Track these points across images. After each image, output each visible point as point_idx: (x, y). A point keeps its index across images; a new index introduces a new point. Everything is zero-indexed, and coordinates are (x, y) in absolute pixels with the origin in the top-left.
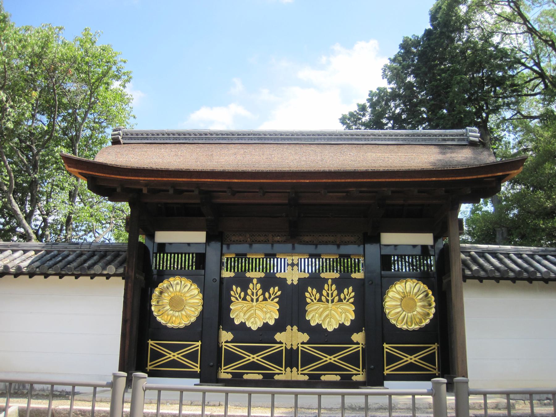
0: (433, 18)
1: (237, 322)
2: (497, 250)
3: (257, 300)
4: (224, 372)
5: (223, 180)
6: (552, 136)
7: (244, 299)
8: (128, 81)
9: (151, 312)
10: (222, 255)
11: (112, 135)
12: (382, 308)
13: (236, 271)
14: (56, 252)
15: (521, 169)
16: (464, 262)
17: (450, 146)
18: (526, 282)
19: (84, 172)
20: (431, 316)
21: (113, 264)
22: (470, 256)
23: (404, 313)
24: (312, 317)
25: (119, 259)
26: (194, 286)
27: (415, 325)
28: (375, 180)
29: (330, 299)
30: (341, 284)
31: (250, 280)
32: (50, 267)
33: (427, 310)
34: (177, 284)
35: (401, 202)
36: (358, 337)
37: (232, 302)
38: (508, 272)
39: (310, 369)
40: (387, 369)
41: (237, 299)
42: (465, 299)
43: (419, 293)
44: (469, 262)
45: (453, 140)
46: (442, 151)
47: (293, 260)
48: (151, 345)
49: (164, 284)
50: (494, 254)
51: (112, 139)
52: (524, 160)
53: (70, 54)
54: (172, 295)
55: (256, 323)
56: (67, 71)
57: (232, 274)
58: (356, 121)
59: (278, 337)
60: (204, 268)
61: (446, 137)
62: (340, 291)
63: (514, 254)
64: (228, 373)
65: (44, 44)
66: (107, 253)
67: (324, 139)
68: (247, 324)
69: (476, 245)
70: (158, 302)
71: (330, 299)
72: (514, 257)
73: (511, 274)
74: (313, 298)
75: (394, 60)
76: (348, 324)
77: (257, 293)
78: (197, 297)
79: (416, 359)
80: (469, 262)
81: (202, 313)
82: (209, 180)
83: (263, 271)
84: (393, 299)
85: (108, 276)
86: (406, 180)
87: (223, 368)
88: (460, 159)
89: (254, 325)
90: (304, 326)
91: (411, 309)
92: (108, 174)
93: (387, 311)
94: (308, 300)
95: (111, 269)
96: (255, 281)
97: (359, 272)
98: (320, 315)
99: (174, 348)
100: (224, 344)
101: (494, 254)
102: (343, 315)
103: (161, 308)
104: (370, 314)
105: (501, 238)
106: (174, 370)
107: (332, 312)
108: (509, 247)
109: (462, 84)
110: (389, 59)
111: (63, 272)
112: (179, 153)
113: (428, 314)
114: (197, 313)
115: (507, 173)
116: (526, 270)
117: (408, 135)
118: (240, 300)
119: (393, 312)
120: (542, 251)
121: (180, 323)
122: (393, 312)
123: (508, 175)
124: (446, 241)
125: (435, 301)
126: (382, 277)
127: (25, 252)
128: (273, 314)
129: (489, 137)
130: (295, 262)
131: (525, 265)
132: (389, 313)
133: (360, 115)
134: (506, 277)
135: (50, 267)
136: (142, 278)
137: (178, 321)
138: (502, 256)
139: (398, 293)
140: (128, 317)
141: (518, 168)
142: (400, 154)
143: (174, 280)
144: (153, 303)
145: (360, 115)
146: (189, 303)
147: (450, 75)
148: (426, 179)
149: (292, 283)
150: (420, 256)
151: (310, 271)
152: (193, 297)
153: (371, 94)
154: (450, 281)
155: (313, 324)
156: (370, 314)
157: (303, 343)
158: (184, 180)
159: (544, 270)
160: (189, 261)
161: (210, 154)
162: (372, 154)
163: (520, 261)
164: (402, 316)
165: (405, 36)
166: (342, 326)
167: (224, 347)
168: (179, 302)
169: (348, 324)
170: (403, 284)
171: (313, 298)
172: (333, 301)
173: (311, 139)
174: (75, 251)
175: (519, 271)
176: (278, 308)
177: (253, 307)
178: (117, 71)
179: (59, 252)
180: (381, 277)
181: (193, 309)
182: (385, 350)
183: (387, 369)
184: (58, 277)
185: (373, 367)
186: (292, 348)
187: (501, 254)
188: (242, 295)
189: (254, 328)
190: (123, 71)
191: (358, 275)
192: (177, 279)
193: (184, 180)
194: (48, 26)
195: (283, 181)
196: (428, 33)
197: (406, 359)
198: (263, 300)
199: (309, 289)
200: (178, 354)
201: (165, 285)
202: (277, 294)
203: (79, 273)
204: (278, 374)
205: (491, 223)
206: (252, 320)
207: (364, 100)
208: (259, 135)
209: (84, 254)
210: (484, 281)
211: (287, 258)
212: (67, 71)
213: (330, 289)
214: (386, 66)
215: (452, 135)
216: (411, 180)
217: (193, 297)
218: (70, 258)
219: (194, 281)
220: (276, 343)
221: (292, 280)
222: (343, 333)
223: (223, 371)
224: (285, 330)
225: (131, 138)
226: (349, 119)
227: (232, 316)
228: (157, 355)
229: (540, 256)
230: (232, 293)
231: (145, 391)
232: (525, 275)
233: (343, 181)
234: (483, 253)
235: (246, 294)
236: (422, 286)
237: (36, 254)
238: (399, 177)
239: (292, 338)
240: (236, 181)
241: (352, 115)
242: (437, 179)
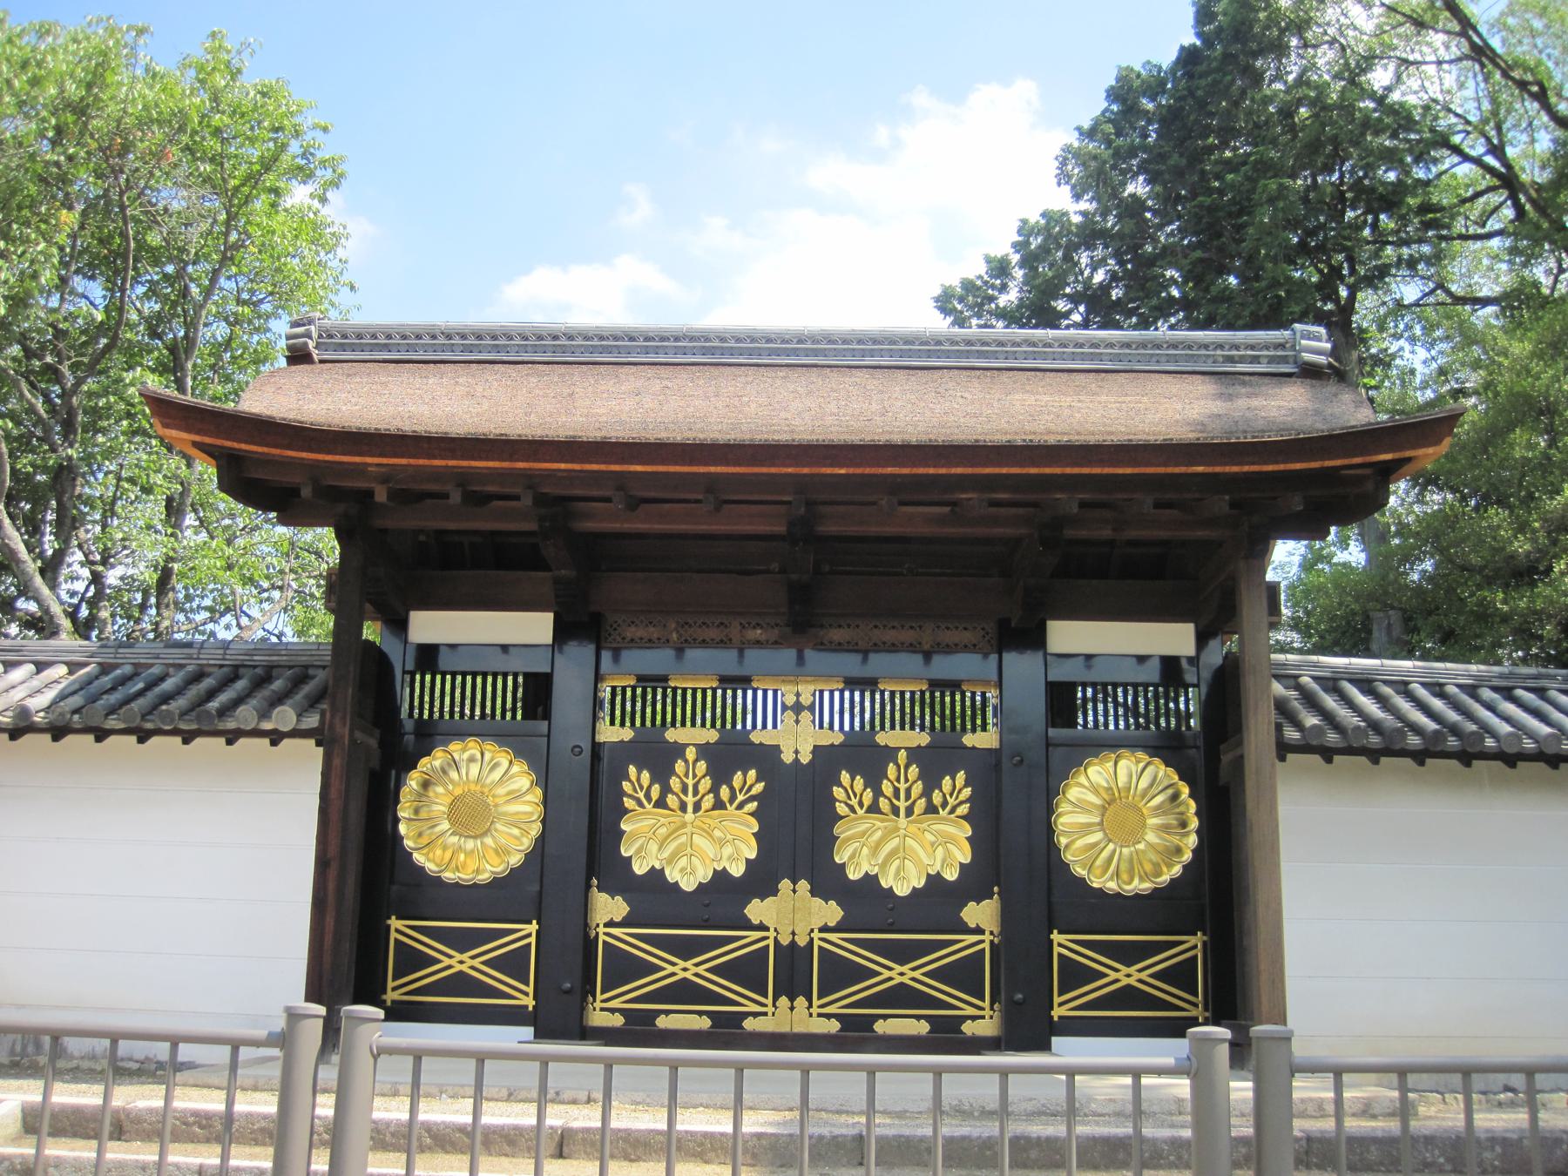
0: (1204, 15)
1: (639, 868)
2: (1376, 671)
3: (697, 807)
4: (602, 1009)
5: (603, 467)
6: (1533, 355)
7: (661, 803)
8: (335, 184)
9: (397, 838)
10: (598, 678)
11: (288, 338)
12: (1050, 831)
13: (638, 723)
14: (128, 669)
15: (1447, 441)
16: (1281, 707)
17: (1247, 378)
18: (1454, 764)
19: (207, 440)
20: (1187, 856)
21: (290, 701)
22: (1299, 687)
23: (1111, 846)
24: (852, 857)
25: (307, 689)
26: (519, 767)
27: (1141, 880)
28: (1034, 471)
29: (902, 805)
30: (935, 762)
31: (678, 750)
32: (112, 711)
33: (1175, 840)
34: (472, 760)
35: (1106, 533)
36: (982, 914)
37: (626, 811)
38: (1404, 736)
39: (843, 1001)
40: (1060, 1005)
41: (640, 804)
42: (1284, 810)
43: (1154, 790)
44: (1296, 704)
45: (1255, 360)
46: (1224, 390)
47: (798, 695)
48: (397, 931)
49: (434, 761)
50: (1366, 684)
51: (289, 348)
52: (1453, 419)
53: (167, 106)
54: (458, 791)
55: (693, 872)
56: (159, 155)
57: (627, 734)
58: (982, 304)
59: (756, 910)
60: (547, 716)
61: (1235, 353)
62: (931, 781)
63: (1423, 684)
64: (613, 1011)
65: (94, 74)
66: (275, 672)
67: (891, 353)
68: (667, 873)
69: (1314, 658)
70: (417, 811)
71: (902, 805)
72: (1422, 693)
73: (1414, 741)
74: (854, 802)
75: (1090, 134)
76: (951, 875)
77: (696, 786)
78: (529, 797)
80: (1296, 704)
81: (541, 841)
82: (563, 466)
83: (713, 725)
84: (1081, 806)
85: (276, 737)
86: (1120, 471)
87: (599, 997)
88: (1274, 413)
89: (688, 875)
90: (829, 882)
91: (1133, 834)
92: (276, 446)
93: (1063, 841)
94: (841, 809)
95: (284, 716)
96: (691, 754)
97: (984, 729)
98: (875, 850)
99: (462, 941)
100: (601, 930)
101: (1366, 684)
102: (940, 851)
103: (424, 826)
104: (1014, 847)
105: (1385, 639)
106: (461, 1003)
107: (910, 843)
108: (1407, 664)
109: (1281, 204)
110: (1079, 129)
111: (149, 726)
112: (479, 389)
113: (1178, 851)
114: (527, 843)
115: (1408, 454)
116: (1454, 730)
117: (1128, 345)
118: (649, 807)
119: (1079, 843)
120: (1501, 676)
121: (478, 871)
122: (1079, 843)
123: (1409, 460)
124: (1232, 644)
125: (1197, 814)
126: (1048, 744)
127: (41, 667)
128: (743, 847)
129: (1355, 355)
130: (806, 700)
131: (1453, 716)
132: (1067, 846)
133: (993, 287)
134: (1398, 747)
135: (112, 711)
136: (373, 743)
137: (472, 865)
138: (1387, 690)
139: (1095, 789)
140: (333, 850)
141: (1438, 442)
142: (1104, 398)
143: (464, 750)
144: (404, 812)
145: (993, 287)
146: (505, 814)
147: (1248, 178)
148: (1177, 470)
149: (797, 760)
150: (1156, 686)
151: (847, 728)
152: (516, 796)
153: (1025, 229)
154: (1242, 757)
155: (853, 875)
156: (1014, 847)
158: (491, 464)
159: (1506, 728)
160: (506, 696)
161: (566, 391)
162: (1026, 396)
163: (1437, 704)
164: (1105, 854)
165: (1124, 65)
166: (935, 881)
167: (602, 938)
168: (475, 811)
169: (951, 875)
170: (1110, 765)
171: (854, 802)
172: (909, 811)
173: (853, 352)
174: (182, 666)
175: (1436, 732)
176: (756, 829)
177: (684, 825)
178: (304, 156)
179: (138, 669)
180: (1048, 745)
181: (516, 832)
182: (1057, 950)
183: (1060, 1005)
184: (134, 739)
185: (1020, 996)
186: (793, 943)
187: (1385, 682)
188: (656, 791)
189: (688, 885)
190: (320, 155)
191: (984, 739)
192: (472, 747)
193: (491, 464)
194: (104, 24)
195: (773, 470)
196: (1189, 57)
197: (1113, 975)
198: (714, 808)
199: (845, 777)
200: (473, 958)
201: (437, 763)
202: (754, 791)
203: (194, 727)
204: (755, 1015)
205: (1357, 598)
206: (683, 862)
207: (1003, 244)
208: (707, 339)
209: (209, 675)
210: (1336, 758)
211: (784, 688)
212: (159, 155)
213: (903, 777)
214: (1067, 149)
215: (1252, 347)
216: (1136, 470)
217: (516, 796)
218: (168, 685)
219: (520, 753)
221: (797, 752)
222: (939, 902)
223: (598, 1005)
224: (775, 892)
225: (343, 347)
226: (961, 300)
228: (412, 960)
229: (1495, 689)
230: (626, 786)
231: (376, 1058)
232: (1453, 742)
233: (943, 471)
234: (1335, 680)
235: (666, 789)
236: (1161, 771)
237: (71, 673)
238: (1101, 463)
239: (794, 914)
240: (639, 468)
241: (968, 286)
242: (1209, 469)
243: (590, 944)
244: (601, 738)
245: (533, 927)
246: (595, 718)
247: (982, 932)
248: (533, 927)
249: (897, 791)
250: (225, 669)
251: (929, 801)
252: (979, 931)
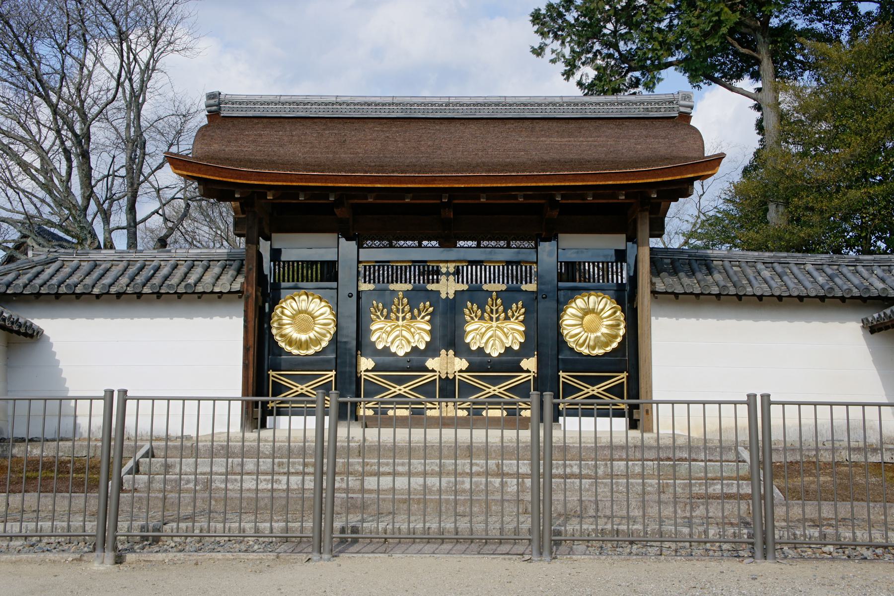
1: (380, 346)
9: (271, 336)
11: (207, 106)
12: (559, 327)
20: (619, 339)
30: (509, 297)
45: (658, 110)
47: (447, 268)
59: (431, 363)
60: (336, 279)
61: (649, 106)
74: (473, 315)
77: (403, 310)
79: (600, 390)
89: (401, 350)
93: (565, 332)
94: (468, 318)
97: (531, 282)
98: (483, 335)
99: (302, 379)
100: (363, 373)
126: (559, 289)
140: (251, 342)
157: (461, 371)
166: (508, 350)
170: (586, 298)
171: (473, 315)
180: (558, 290)
186: (447, 377)
191: (532, 287)
197: (586, 390)
218: (165, 271)
224: (439, 355)
238: (569, 181)
243: (358, 379)
244: (361, 289)
245: (333, 373)
246: (358, 280)
247: (530, 372)
248: (333, 373)
249: (492, 311)
250: (188, 262)
251: (506, 314)
252: (528, 371)
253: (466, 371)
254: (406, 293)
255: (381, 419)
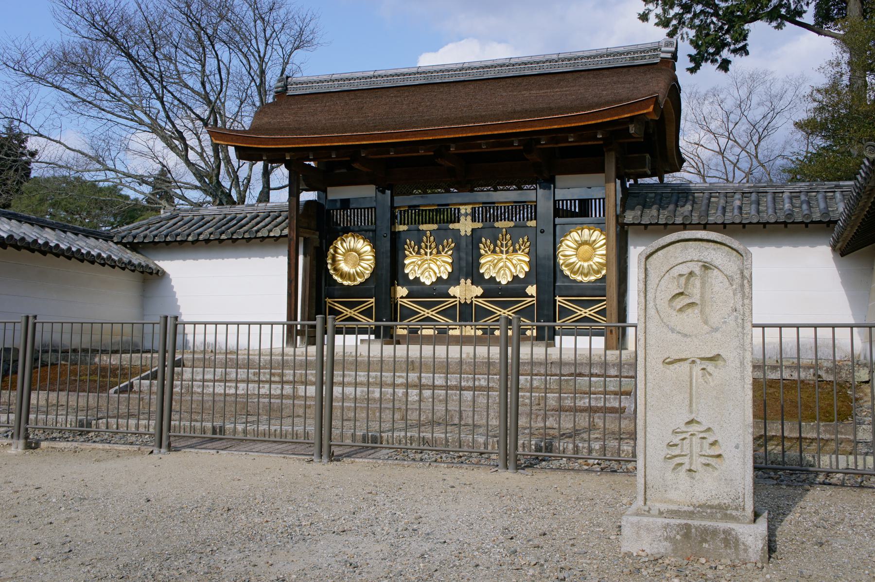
3: (431, 253)
12: (555, 257)
45: (643, 58)
59: (453, 291)
79: (591, 313)
89: (428, 280)
90: (477, 279)
93: (561, 262)
94: (482, 252)
96: (428, 233)
107: (506, 265)
157: (477, 297)
189: (428, 283)
220: (450, 297)
224: (459, 284)
227: (406, 271)
238: (519, 127)
239: (465, 291)
245: (373, 300)
248: (373, 300)
252: (532, 296)
253: (407, 297)
254: (508, 230)
255: (414, 336)
